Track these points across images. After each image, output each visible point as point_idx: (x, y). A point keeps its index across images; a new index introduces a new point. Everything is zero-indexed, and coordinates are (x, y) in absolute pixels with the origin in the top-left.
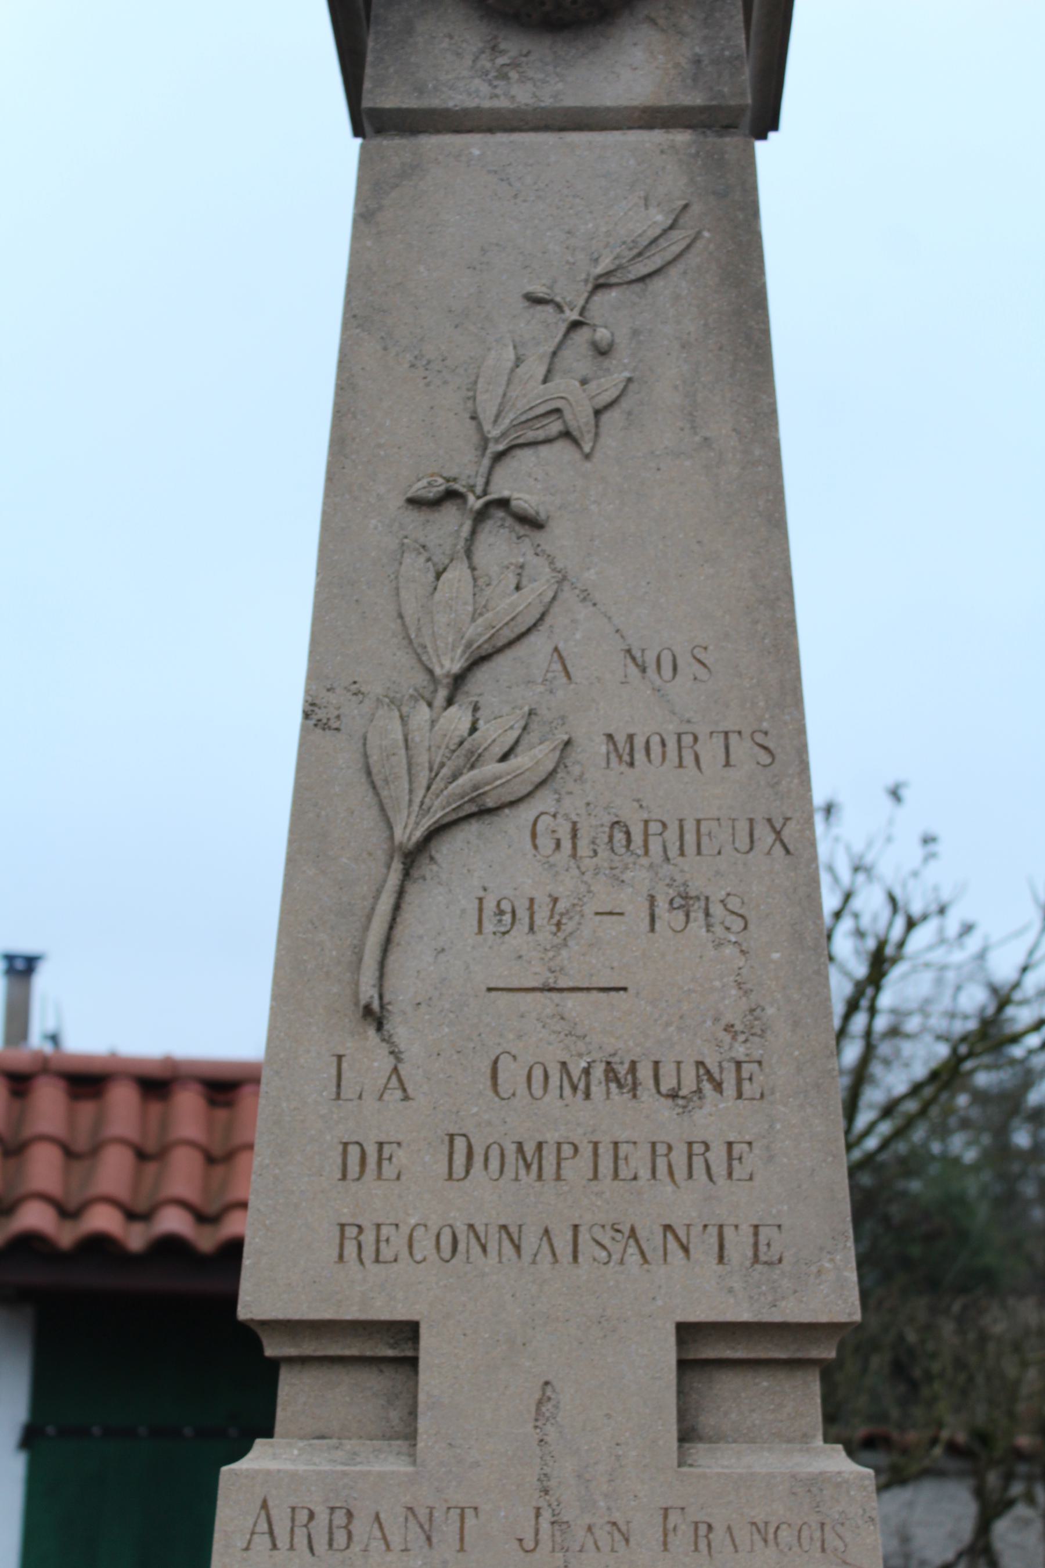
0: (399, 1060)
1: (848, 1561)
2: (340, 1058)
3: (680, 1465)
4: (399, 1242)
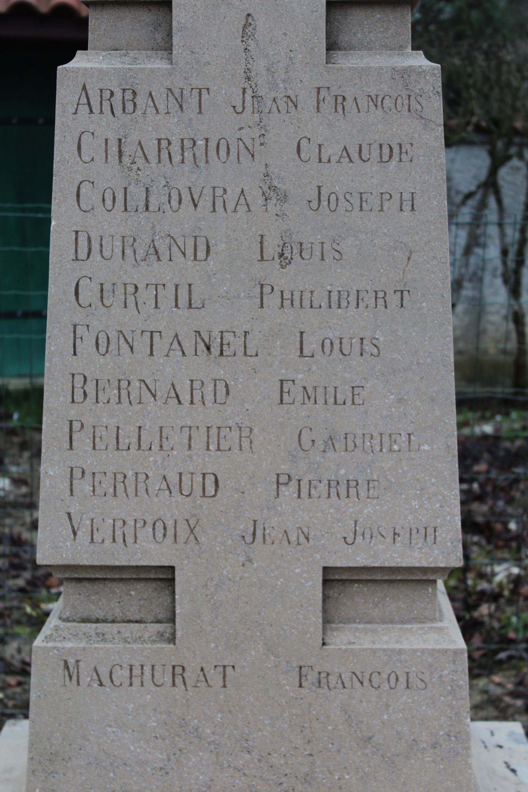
1: (424, 116)
3: (327, 63)
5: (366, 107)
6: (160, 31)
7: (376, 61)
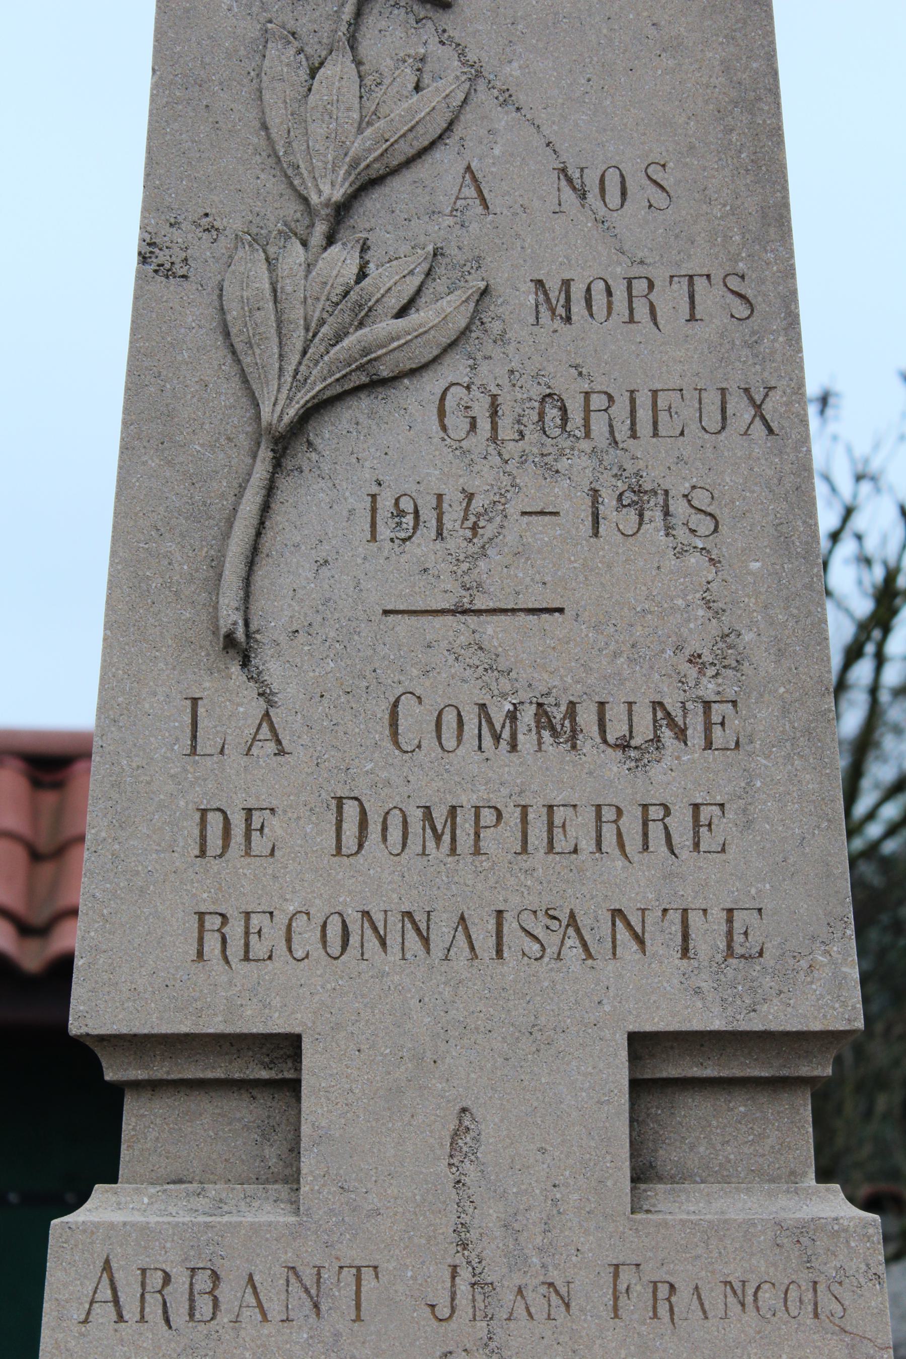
0: (271, 703)
1: (848, 1328)
2: (195, 701)
3: (632, 1213)
4: (274, 935)
5: (721, 1306)
6: (275, 1141)
7: (740, 1205)
